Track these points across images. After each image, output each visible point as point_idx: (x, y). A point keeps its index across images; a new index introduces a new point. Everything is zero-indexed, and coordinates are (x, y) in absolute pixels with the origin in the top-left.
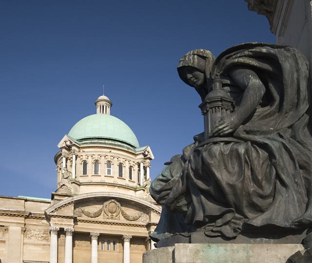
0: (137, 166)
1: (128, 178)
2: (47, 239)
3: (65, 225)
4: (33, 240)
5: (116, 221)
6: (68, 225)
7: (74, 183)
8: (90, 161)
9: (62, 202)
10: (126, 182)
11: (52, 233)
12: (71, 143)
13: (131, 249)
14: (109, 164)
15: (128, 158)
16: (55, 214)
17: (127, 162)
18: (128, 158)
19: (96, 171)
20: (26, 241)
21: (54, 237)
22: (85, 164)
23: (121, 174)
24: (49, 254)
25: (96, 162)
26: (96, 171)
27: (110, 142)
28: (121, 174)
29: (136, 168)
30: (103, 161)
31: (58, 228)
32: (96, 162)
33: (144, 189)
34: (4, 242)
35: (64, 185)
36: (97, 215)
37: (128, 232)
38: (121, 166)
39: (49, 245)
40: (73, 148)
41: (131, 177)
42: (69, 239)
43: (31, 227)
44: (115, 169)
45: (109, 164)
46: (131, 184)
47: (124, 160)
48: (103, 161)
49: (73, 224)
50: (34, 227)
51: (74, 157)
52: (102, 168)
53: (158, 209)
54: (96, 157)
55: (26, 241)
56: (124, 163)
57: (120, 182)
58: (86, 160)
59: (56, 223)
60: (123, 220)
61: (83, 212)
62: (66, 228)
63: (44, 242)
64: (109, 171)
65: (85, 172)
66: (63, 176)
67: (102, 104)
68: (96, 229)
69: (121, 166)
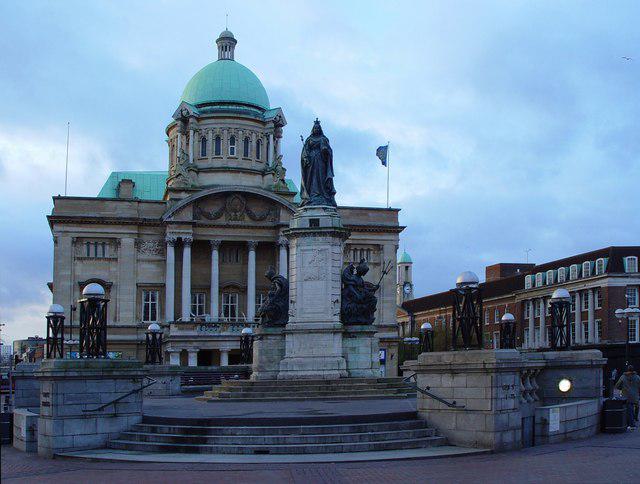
2: (163, 252)
4: (147, 256)
5: (240, 223)
6: (187, 234)
8: (210, 137)
9: (180, 203)
10: (254, 165)
13: (257, 259)
14: (233, 140)
16: (172, 219)
19: (218, 152)
20: (141, 256)
21: (171, 252)
22: (204, 141)
23: (246, 154)
24: (164, 273)
25: (218, 139)
26: (218, 152)
27: (234, 107)
28: (246, 154)
29: (265, 141)
30: (225, 137)
32: (218, 139)
34: (116, 259)
36: (218, 216)
37: (253, 237)
38: (247, 141)
39: (165, 261)
40: (191, 120)
42: (187, 252)
43: (145, 238)
44: (239, 146)
45: (233, 140)
48: (225, 137)
49: (191, 231)
50: (149, 238)
51: (191, 132)
52: (225, 145)
54: (218, 131)
55: (141, 256)
57: (246, 165)
59: (171, 234)
60: (247, 221)
62: (183, 237)
63: (159, 258)
64: (232, 153)
65: (204, 153)
68: (216, 236)
69: (247, 141)
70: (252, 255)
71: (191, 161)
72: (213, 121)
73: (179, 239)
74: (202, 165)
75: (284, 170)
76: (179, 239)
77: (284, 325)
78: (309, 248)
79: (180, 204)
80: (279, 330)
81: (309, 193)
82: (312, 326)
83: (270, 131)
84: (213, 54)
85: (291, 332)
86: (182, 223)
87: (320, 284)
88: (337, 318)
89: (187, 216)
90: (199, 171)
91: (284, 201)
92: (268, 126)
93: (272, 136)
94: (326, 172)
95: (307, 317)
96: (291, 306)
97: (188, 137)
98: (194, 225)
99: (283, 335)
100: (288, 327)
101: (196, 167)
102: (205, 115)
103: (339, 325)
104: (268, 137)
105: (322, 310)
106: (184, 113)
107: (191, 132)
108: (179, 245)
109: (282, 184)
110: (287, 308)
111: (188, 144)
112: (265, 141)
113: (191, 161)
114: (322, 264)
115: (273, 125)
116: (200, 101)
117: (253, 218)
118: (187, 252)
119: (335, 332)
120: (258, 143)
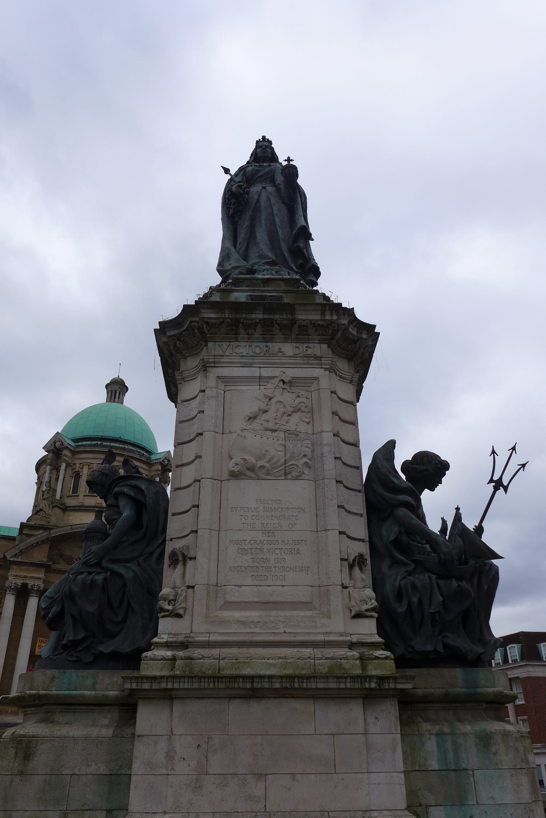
3: (31, 577)
7: (56, 506)
9: (33, 539)
11: (8, 592)
12: (62, 444)
22: (77, 476)
31: (19, 582)
35: (41, 510)
40: (66, 452)
49: (42, 575)
51: (63, 466)
58: (80, 470)
61: (61, 556)
62: (30, 583)
66: (43, 496)
67: (114, 389)
71: (58, 496)
72: (90, 455)
73: (24, 586)
74: (71, 502)
76: (24, 586)
77: (133, 660)
78: (255, 372)
79: (32, 540)
80: (108, 684)
81: (245, 257)
82: (264, 663)
83: (156, 473)
84: (102, 397)
85: (166, 695)
86: (32, 565)
87: (294, 493)
88: (368, 629)
89: (40, 555)
90: (65, 509)
94: (292, 220)
95: (238, 623)
96: (171, 579)
97: (58, 472)
98: (47, 568)
99: (126, 708)
100: (155, 662)
101: (63, 504)
102: (81, 449)
103: (383, 663)
105: (303, 595)
106: (58, 444)
107: (63, 466)
108: (23, 594)
110: (151, 588)
111: (57, 479)
113: (58, 496)
114: (295, 422)
115: (160, 468)
116: (78, 435)
118: (33, 603)
119: (369, 694)
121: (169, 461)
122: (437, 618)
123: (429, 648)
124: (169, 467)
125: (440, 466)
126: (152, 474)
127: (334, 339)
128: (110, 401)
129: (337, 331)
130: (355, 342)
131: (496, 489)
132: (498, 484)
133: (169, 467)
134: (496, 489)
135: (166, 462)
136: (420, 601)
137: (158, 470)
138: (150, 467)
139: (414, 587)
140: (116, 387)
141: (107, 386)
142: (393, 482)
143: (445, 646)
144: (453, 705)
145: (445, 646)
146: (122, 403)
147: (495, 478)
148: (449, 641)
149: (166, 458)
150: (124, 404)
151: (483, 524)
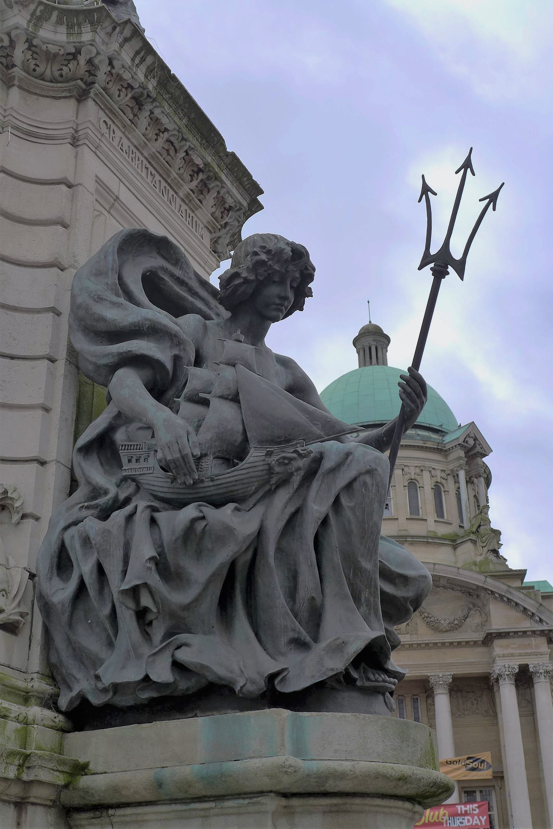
0: (451, 480)
1: (432, 517)
10: (430, 525)
15: (428, 464)
17: (426, 474)
18: (428, 464)
23: (414, 508)
28: (414, 508)
33: (473, 537)
38: (413, 486)
41: (440, 512)
46: (442, 530)
47: (418, 470)
53: (505, 587)
56: (418, 478)
57: (416, 529)
67: (366, 344)
70: (442, 702)
75: (497, 533)
83: (457, 464)
84: (350, 360)
91: (499, 586)
92: (452, 456)
93: (462, 475)
104: (456, 478)
109: (492, 557)
112: (450, 486)
115: (462, 453)
117: (434, 626)
120: (438, 490)
121: (475, 439)
122: (146, 601)
123: (132, 674)
124: (478, 449)
125: (264, 257)
126: (451, 467)
127: (14, 66)
128: (365, 365)
129: (12, 44)
130: (75, 55)
131: (439, 274)
132: (442, 263)
133: (478, 449)
134: (439, 274)
135: (471, 442)
136: (101, 571)
137: (460, 458)
138: (446, 456)
139: (86, 541)
140: (369, 341)
141: (355, 342)
142: (103, 319)
143: (178, 666)
144: (193, 806)
145: (178, 666)
146: (385, 363)
147: (434, 251)
148: (183, 655)
149: (468, 436)
150: (389, 365)
151: (422, 371)
